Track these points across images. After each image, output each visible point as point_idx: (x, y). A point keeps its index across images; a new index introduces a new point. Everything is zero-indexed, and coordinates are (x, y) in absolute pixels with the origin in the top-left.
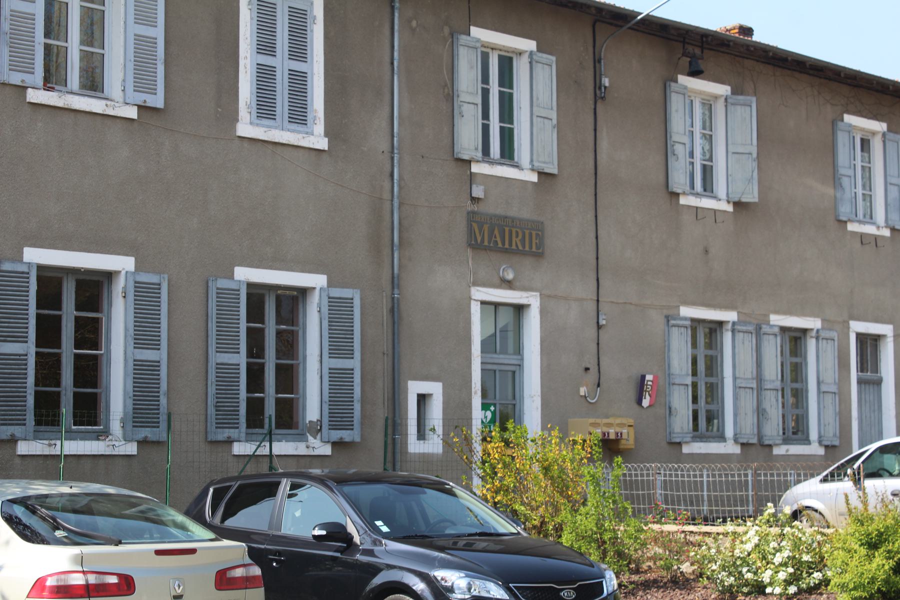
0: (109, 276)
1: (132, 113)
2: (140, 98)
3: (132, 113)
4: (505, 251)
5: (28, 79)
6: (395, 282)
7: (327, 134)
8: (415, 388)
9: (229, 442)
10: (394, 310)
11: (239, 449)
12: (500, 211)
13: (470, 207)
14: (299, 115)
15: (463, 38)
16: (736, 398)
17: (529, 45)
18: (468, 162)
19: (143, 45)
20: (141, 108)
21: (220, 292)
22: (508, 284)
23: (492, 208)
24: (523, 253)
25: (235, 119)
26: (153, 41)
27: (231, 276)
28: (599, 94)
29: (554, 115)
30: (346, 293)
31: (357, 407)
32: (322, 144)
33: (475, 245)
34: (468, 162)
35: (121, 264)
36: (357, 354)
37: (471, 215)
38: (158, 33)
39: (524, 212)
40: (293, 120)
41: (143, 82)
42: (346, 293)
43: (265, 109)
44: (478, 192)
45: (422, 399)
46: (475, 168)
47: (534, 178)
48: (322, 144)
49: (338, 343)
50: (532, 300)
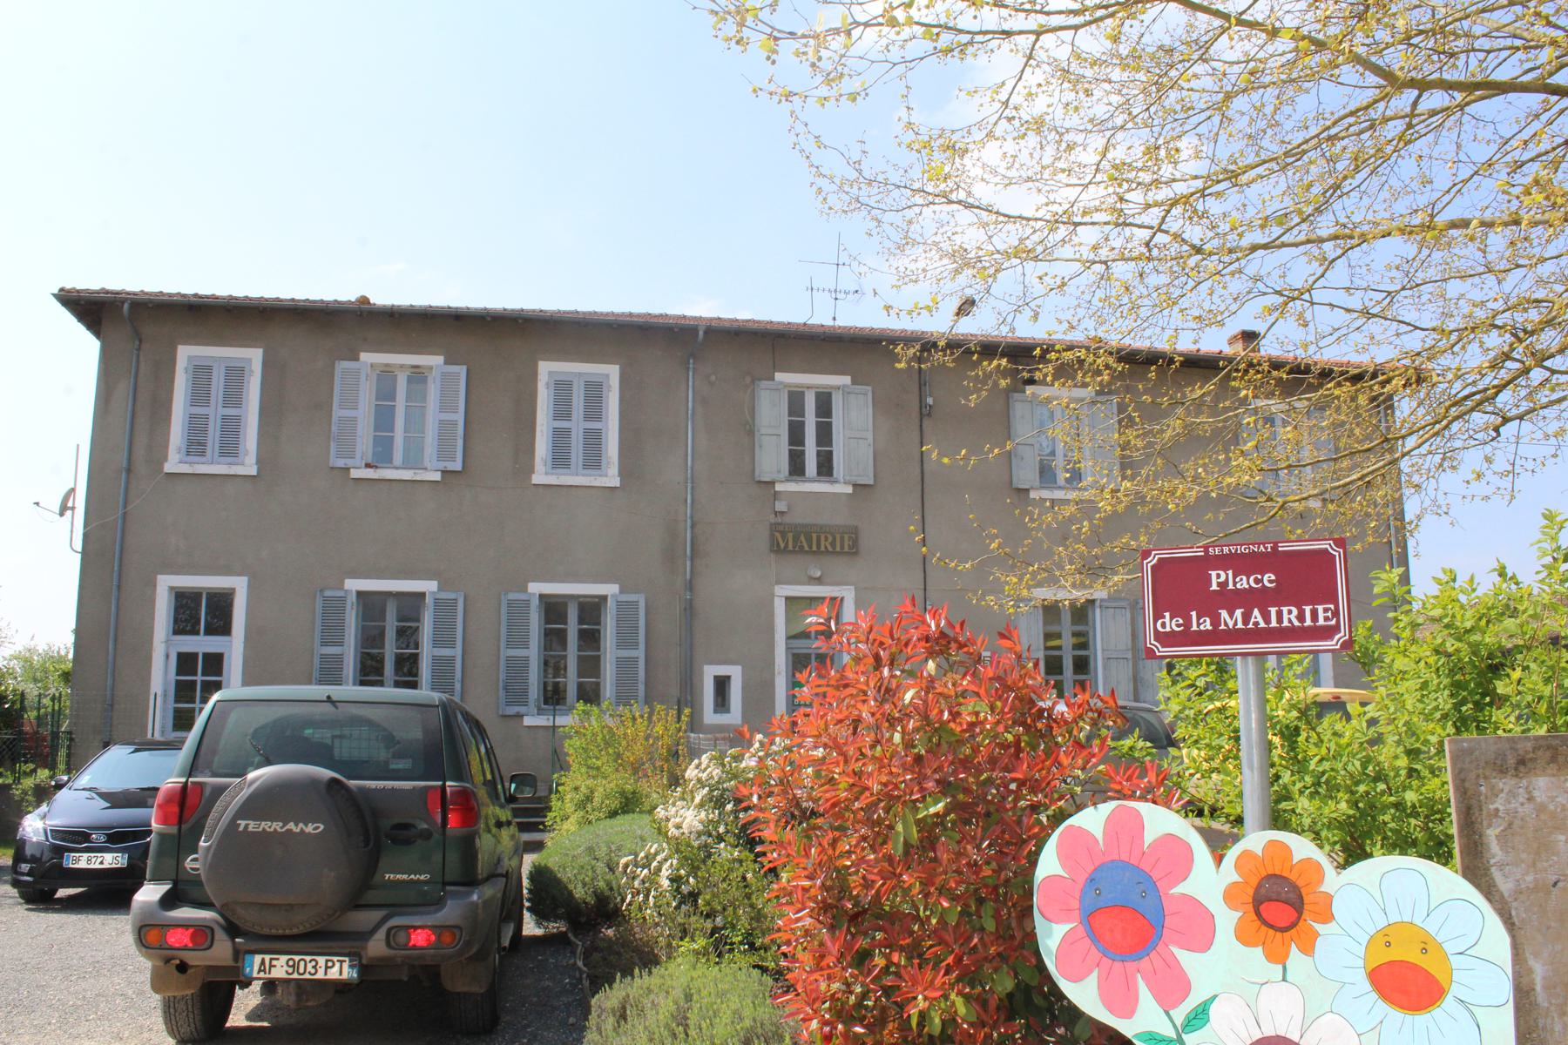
0: (421, 596)
1: (437, 477)
2: (442, 465)
3: (437, 477)
4: (818, 553)
5: (350, 462)
6: (690, 586)
7: (621, 474)
8: (710, 672)
9: (520, 716)
10: (690, 610)
11: (528, 721)
12: (808, 520)
13: (772, 519)
14: (593, 460)
15: (764, 384)
16: (1105, 668)
17: (846, 380)
18: (773, 483)
19: (445, 428)
20: (444, 472)
21: (510, 604)
22: (819, 581)
23: (798, 517)
24: (834, 553)
25: (531, 470)
26: (455, 423)
27: (525, 590)
28: (925, 412)
29: (870, 436)
30: (632, 597)
31: (641, 687)
32: (616, 482)
33: (777, 549)
34: (773, 483)
35: (429, 586)
36: (642, 646)
37: (774, 527)
38: (460, 417)
39: (840, 519)
40: (223, 454)
41: (444, 452)
42: (632, 597)
43: (560, 459)
44: (781, 506)
45: (722, 684)
46: (779, 487)
47: (849, 490)
48: (616, 482)
49: (625, 641)
50: (848, 594)
